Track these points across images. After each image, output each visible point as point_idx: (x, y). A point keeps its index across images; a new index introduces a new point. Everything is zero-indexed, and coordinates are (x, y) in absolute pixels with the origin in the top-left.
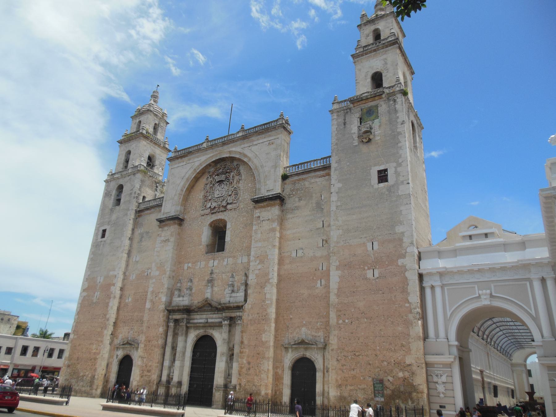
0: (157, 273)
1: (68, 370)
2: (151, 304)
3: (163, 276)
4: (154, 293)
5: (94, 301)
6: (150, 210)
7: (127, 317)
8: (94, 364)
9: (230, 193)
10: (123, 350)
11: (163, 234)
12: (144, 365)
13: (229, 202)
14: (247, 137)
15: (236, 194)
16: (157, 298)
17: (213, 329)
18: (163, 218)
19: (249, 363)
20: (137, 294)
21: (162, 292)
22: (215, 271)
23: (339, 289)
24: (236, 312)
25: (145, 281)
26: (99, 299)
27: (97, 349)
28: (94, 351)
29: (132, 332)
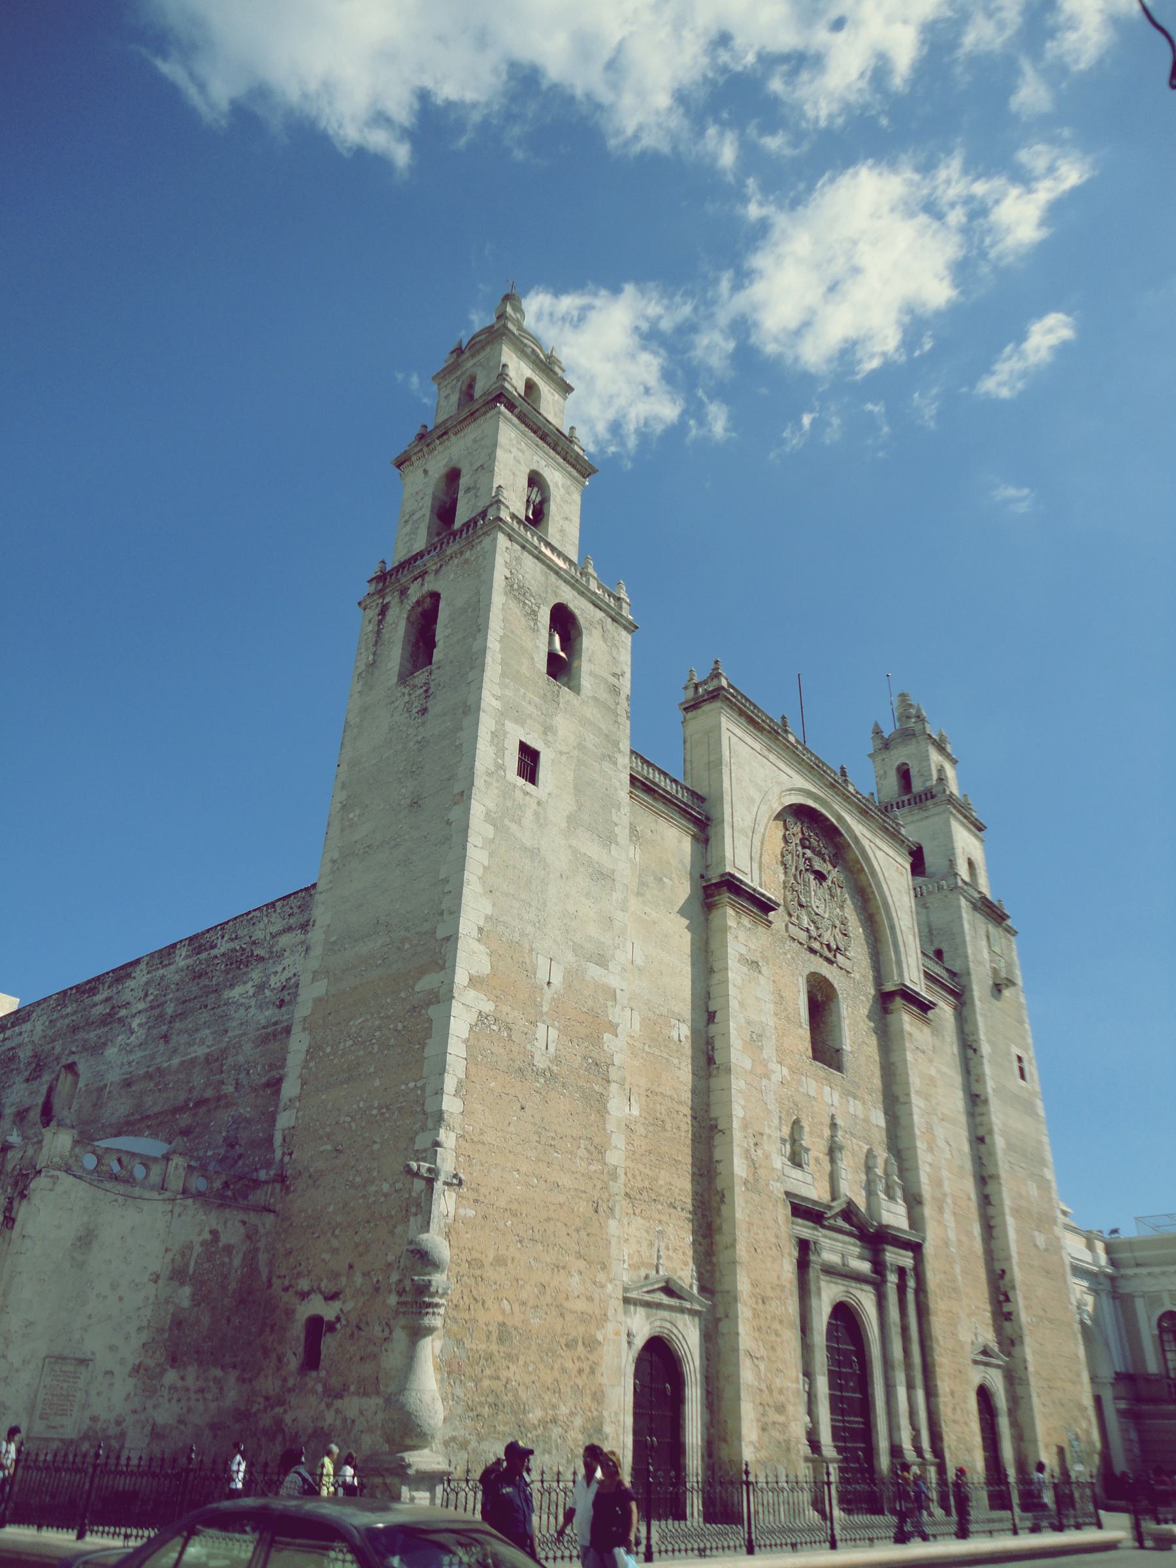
0: (748, 1064)
1: (459, 1392)
2: (749, 1166)
3: (764, 1082)
4: (750, 1131)
5: (541, 1062)
6: (655, 799)
7: (634, 1176)
8: (586, 1366)
9: (837, 923)
10: (648, 1318)
11: (742, 935)
12: (763, 1386)
13: (840, 945)
14: (867, 813)
15: (845, 935)
16: (760, 1152)
17: (862, 1290)
18: (746, 885)
19: (952, 1393)
20: (659, 1098)
21: (770, 1136)
22: (839, 1121)
23: (1019, 1253)
24: (904, 1256)
25: (676, 1061)
26: (557, 1060)
27: (590, 1299)
28: (580, 1305)
29: (663, 1245)
